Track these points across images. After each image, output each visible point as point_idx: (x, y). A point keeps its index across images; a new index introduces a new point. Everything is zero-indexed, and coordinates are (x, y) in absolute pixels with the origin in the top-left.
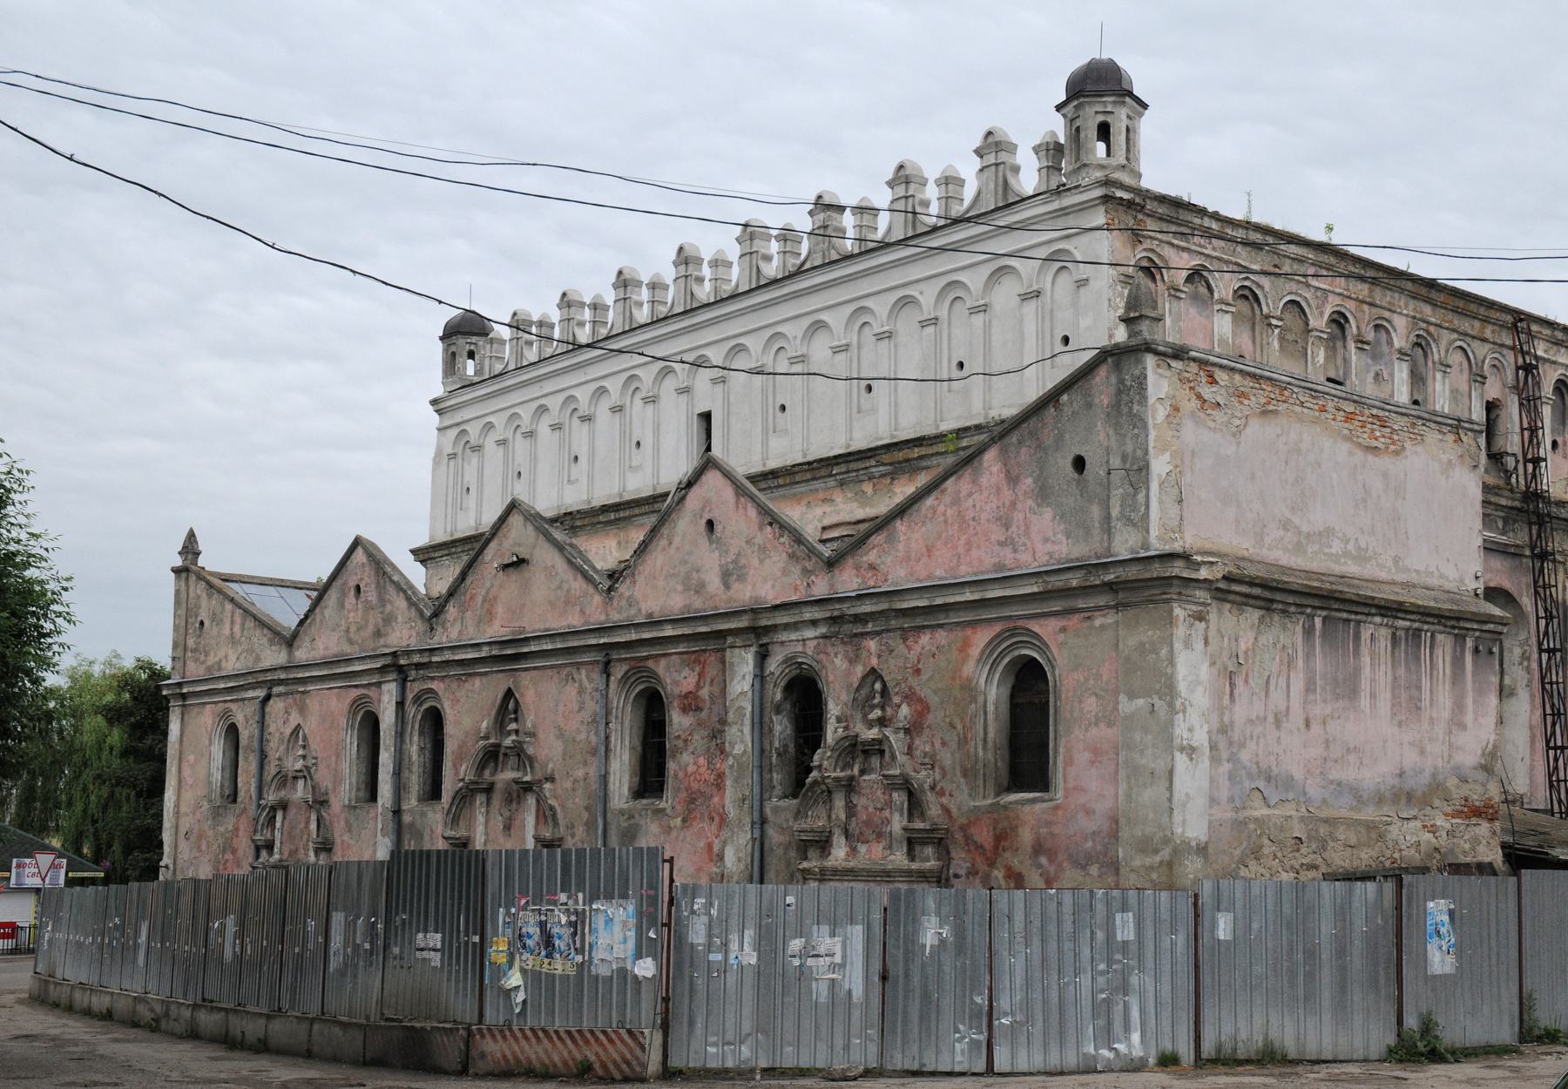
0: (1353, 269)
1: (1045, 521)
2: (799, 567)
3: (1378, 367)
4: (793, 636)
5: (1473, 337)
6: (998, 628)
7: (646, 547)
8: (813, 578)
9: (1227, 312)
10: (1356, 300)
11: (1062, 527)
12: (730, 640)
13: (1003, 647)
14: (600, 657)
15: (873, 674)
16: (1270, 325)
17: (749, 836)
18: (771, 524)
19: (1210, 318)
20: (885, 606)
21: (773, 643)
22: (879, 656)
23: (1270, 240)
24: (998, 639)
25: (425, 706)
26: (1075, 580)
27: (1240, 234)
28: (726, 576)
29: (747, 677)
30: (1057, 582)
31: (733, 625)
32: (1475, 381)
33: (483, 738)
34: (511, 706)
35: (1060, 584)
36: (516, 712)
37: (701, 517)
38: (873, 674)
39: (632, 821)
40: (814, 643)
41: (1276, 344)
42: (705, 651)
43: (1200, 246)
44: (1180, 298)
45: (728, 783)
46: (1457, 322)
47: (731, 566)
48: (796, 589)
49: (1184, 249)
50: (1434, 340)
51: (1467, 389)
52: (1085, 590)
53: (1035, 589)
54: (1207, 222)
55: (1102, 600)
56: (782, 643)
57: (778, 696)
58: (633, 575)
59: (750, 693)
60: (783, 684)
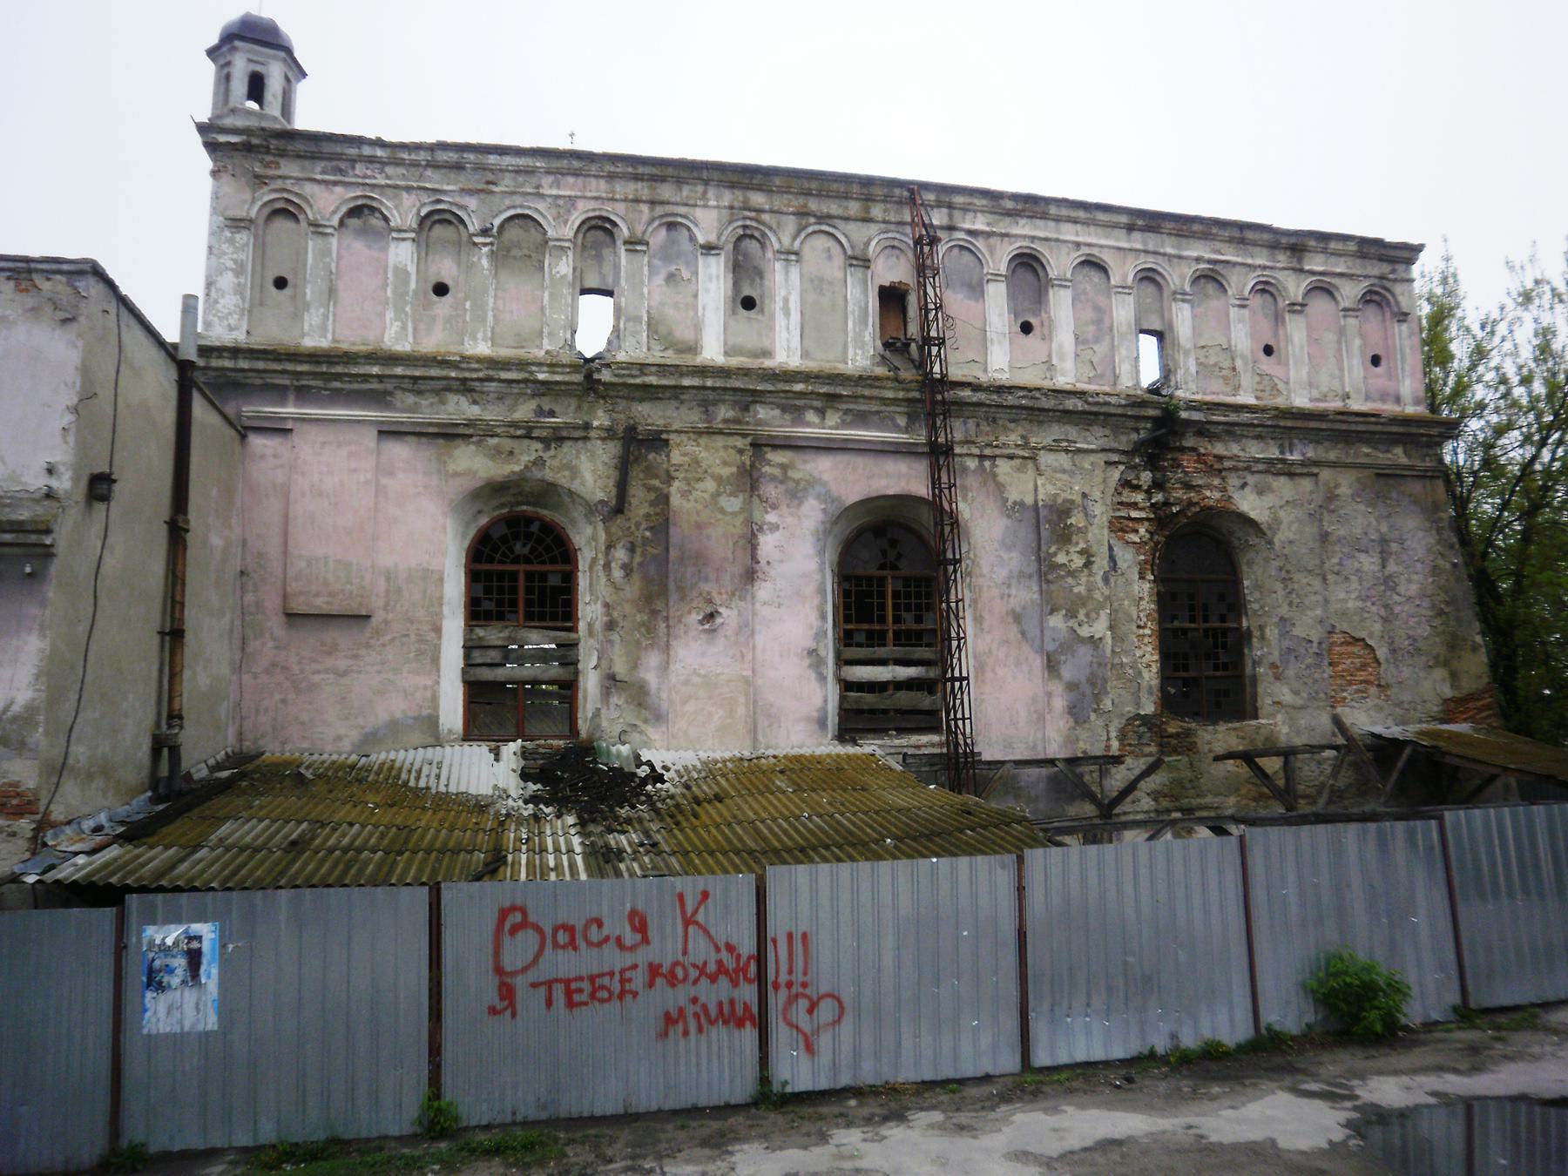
0: (612, 169)
3: (673, 268)
5: (847, 219)
9: (404, 240)
10: (626, 200)
16: (475, 244)
19: (385, 249)
23: (471, 157)
27: (422, 156)
32: (851, 265)
41: (485, 262)
43: (369, 177)
44: (326, 234)
46: (813, 205)
49: (335, 183)
50: (770, 228)
51: (841, 275)
54: (367, 151)
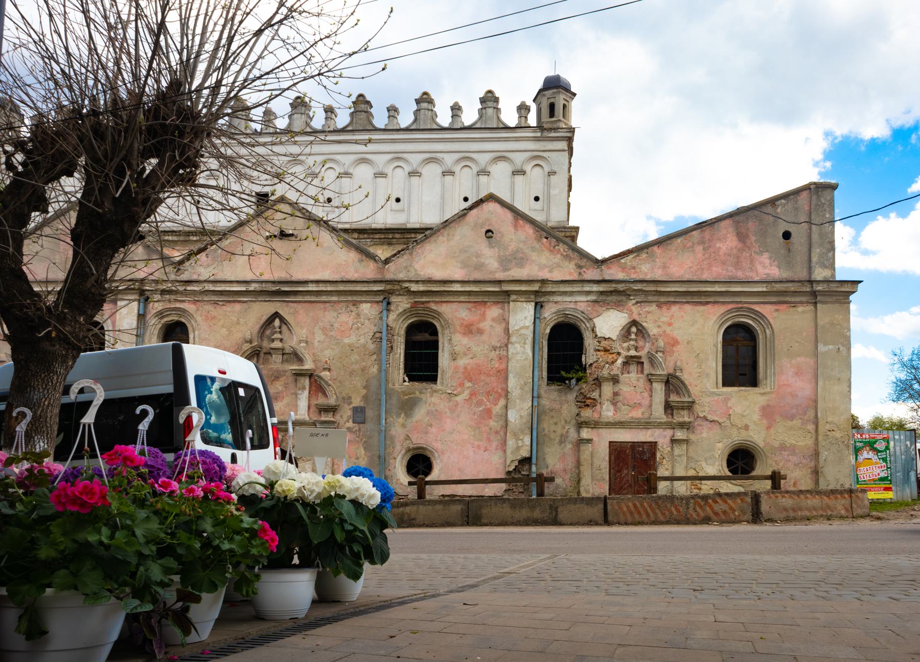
1: (765, 258)
2: (573, 263)
4: (568, 299)
6: (730, 306)
7: (427, 238)
8: (584, 269)
11: (776, 263)
12: (513, 297)
13: (730, 315)
14: (380, 298)
15: (634, 323)
17: (530, 404)
18: (547, 238)
20: (653, 289)
21: (549, 302)
22: (640, 314)
24: (729, 311)
25: (166, 319)
26: (792, 287)
28: (505, 263)
29: (529, 318)
30: (779, 287)
31: (524, 288)
33: (247, 342)
34: (277, 322)
35: (783, 289)
36: (280, 327)
37: (482, 227)
38: (634, 323)
39: (412, 396)
40: (586, 304)
42: (486, 302)
45: (511, 376)
47: (510, 258)
48: (571, 274)
52: (795, 293)
53: (765, 289)
55: (804, 299)
56: (556, 302)
57: (548, 331)
58: (411, 254)
59: (532, 327)
60: (552, 325)
